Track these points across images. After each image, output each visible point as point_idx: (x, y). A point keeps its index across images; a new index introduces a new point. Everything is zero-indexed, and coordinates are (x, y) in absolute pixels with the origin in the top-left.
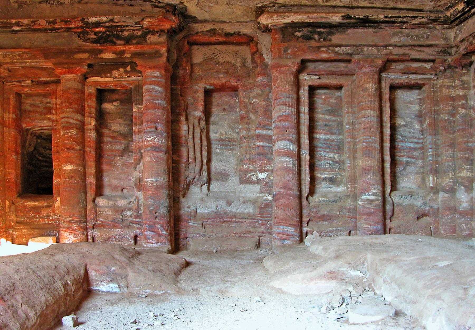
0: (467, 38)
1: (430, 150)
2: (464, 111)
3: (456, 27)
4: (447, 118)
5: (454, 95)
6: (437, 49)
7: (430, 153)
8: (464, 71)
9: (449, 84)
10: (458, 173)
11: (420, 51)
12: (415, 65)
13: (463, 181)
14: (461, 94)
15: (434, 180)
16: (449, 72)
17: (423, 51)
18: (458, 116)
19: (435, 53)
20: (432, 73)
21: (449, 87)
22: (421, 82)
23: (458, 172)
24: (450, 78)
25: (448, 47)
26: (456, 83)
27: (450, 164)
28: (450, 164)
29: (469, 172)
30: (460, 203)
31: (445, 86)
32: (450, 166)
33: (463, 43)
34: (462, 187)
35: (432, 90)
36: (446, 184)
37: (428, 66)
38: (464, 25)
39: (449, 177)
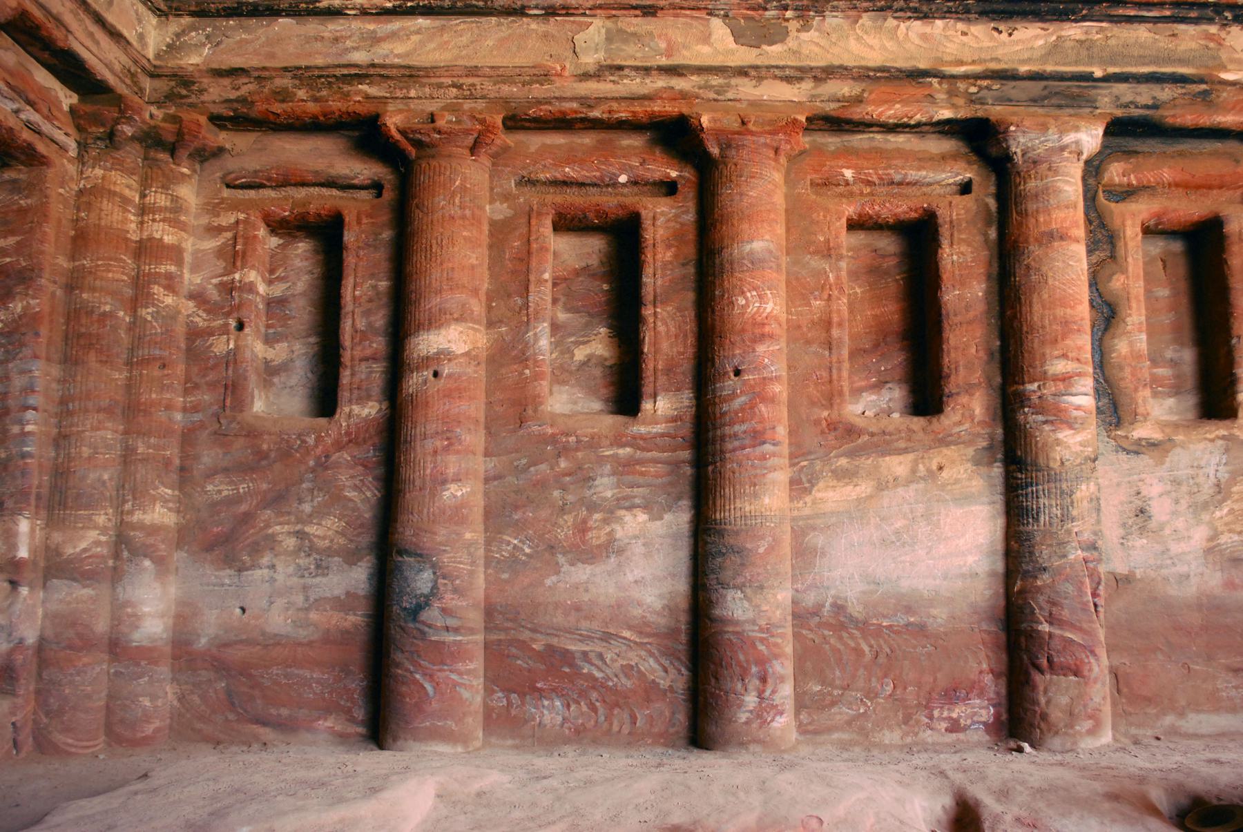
0: (267, 74)
1: (30, 414)
2: (169, 300)
3: (186, 20)
4: (108, 308)
5: (135, 237)
6: (124, 59)
7: (29, 428)
8: (185, 170)
9: (127, 192)
10: (131, 512)
11: (91, 35)
12: (43, 77)
13: (151, 540)
14: (168, 239)
15: (32, 530)
16: (132, 154)
17: (98, 43)
18: (146, 313)
19: (117, 67)
20: (70, 131)
21: (126, 201)
22: (41, 147)
23: (128, 506)
24: (131, 173)
25: (143, 69)
26: (150, 199)
27: (106, 477)
28: (106, 477)
29: (170, 509)
30: (136, 619)
31: (115, 193)
32: (104, 483)
33: (226, 82)
34: (147, 563)
35: (61, 190)
36: (85, 550)
37: (67, 98)
38: (247, 30)
39: (96, 528)
